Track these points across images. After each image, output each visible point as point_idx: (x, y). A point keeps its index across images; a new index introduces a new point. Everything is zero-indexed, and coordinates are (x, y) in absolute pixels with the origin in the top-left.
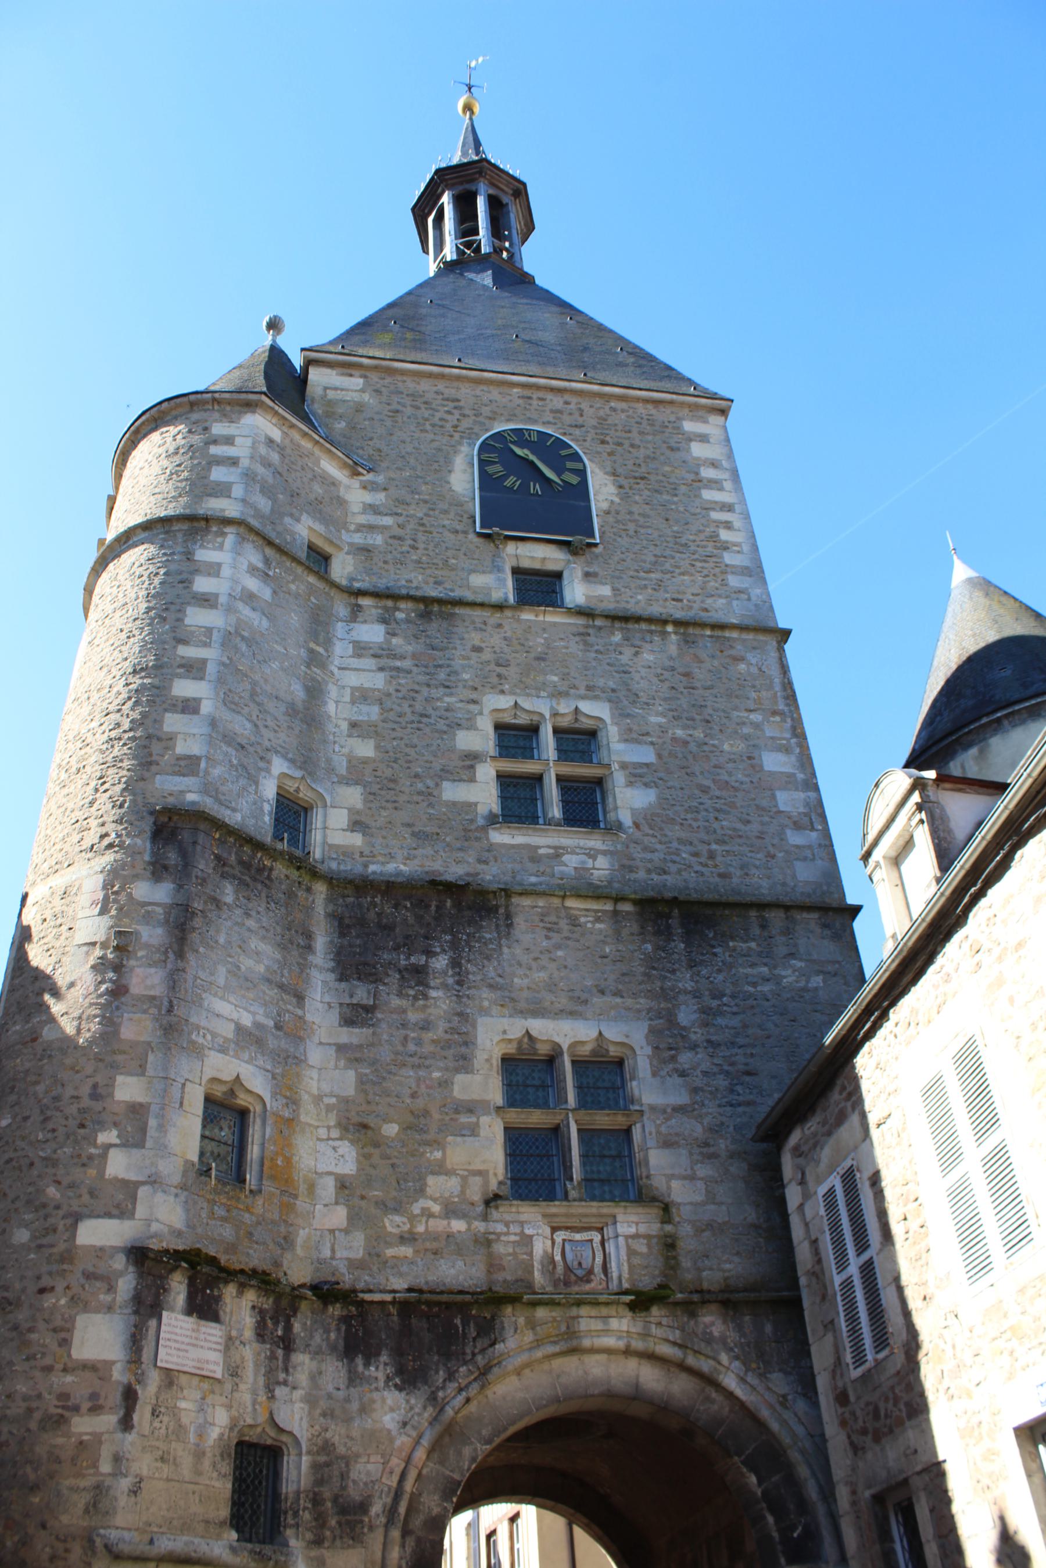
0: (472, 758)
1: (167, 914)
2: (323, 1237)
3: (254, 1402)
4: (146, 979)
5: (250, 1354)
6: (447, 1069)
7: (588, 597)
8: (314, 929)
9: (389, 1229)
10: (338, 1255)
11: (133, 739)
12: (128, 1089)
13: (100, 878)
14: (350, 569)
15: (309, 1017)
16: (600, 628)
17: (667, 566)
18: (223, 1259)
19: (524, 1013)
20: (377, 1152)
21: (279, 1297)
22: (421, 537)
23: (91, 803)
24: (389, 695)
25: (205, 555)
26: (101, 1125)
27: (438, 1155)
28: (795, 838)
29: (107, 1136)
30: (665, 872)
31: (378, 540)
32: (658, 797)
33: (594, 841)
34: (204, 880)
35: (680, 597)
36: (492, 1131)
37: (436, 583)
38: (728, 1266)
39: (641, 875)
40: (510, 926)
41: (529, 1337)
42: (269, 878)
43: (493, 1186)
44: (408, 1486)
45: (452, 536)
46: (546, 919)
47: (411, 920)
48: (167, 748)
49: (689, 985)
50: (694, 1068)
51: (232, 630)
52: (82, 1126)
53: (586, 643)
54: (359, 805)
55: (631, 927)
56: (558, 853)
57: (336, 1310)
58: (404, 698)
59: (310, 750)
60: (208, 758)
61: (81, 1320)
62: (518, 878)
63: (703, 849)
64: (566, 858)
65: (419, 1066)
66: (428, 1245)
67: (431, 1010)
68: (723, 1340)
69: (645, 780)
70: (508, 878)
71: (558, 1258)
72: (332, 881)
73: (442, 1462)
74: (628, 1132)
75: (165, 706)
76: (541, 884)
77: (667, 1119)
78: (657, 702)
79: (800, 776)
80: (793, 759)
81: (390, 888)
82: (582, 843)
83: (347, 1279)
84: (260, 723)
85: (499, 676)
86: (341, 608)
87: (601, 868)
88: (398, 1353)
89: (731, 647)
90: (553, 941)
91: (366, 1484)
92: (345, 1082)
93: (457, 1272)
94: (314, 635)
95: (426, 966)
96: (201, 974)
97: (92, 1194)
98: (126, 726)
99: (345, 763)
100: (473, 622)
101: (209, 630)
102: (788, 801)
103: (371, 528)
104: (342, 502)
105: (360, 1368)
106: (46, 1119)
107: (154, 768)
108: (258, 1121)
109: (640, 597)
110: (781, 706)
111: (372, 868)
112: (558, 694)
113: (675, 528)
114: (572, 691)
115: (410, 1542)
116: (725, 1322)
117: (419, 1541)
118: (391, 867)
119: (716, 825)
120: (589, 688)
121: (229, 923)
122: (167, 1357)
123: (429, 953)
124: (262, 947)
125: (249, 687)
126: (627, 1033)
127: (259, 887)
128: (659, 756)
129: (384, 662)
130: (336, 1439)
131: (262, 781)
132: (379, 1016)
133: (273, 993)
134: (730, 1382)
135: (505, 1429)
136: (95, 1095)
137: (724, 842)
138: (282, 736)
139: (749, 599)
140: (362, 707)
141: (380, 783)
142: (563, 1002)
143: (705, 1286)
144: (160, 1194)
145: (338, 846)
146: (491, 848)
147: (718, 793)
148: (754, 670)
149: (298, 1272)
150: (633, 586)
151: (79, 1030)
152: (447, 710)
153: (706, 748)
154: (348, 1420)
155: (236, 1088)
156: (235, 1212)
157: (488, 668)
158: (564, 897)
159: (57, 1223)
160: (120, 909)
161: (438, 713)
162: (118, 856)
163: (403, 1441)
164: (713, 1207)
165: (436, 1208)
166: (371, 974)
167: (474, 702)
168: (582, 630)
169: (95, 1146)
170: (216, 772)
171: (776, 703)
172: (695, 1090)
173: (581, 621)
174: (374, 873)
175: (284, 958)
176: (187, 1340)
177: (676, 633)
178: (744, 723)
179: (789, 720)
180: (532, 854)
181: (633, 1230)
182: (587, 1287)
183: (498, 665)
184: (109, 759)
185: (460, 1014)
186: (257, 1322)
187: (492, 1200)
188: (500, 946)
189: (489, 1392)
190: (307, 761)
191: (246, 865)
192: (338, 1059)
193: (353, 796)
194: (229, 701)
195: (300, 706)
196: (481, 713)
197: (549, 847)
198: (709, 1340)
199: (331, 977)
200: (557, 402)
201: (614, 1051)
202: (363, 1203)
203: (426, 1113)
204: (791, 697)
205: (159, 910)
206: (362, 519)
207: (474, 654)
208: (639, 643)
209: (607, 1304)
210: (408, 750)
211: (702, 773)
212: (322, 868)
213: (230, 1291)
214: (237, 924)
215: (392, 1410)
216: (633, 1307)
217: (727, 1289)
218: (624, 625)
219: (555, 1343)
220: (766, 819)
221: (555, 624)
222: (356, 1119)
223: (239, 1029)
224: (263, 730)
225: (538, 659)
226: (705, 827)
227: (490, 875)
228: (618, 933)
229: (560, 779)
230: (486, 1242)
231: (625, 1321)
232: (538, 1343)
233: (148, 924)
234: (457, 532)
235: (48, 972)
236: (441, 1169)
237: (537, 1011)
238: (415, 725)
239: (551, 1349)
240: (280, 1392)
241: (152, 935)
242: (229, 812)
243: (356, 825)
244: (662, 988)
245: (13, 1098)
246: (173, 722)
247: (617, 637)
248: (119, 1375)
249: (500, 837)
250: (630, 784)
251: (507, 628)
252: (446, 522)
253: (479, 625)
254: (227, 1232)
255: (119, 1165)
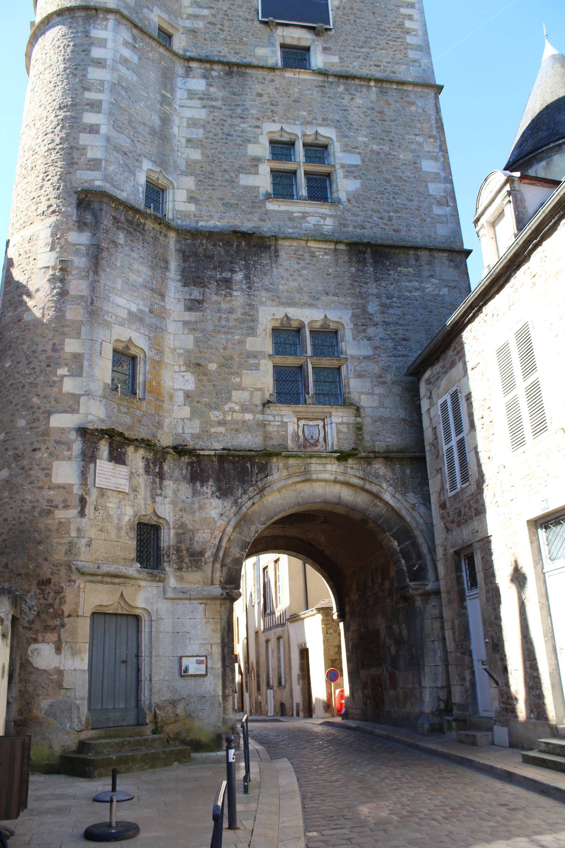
0: (256, 161)
1: (88, 250)
2: (178, 422)
3: (145, 504)
4: (78, 286)
5: (142, 481)
6: (243, 334)
7: (325, 63)
8: (169, 258)
9: (213, 418)
10: (186, 431)
11: (63, 149)
12: (71, 346)
13: (49, 231)
14: (184, 43)
15: (167, 307)
16: (332, 83)
17: (373, 44)
18: (126, 434)
19: (284, 304)
20: (205, 378)
21: (156, 452)
22: (226, 23)
23: (41, 188)
24: (209, 123)
26: (59, 365)
27: (238, 380)
28: (437, 211)
29: (63, 371)
30: (364, 228)
31: (200, 25)
32: (362, 185)
33: (325, 209)
34: (107, 231)
35: (379, 64)
36: (267, 368)
37: (235, 53)
38: (389, 439)
39: (351, 229)
40: (277, 256)
41: (285, 473)
42: (143, 229)
43: (267, 396)
44: (224, 544)
45: (245, 23)
46: (297, 253)
47: (223, 253)
48: (82, 155)
49: (375, 291)
50: (375, 336)
51: (116, 83)
52: (49, 366)
53: (323, 92)
54: (193, 188)
56: (304, 215)
57: (185, 459)
58: (217, 124)
59: (164, 155)
60: (106, 160)
61: (55, 464)
62: (282, 230)
63: (386, 215)
64: (309, 219)
65: (228, 333)
66: (233, 426)
67: (233, 303)
68: (385, 477)
69: (355, 175)
70: (276, 230)
71: (301, 434)
72: (178, 230)
73: (240, 533)
74: (339, 369)
75: (79, 129)
76: (294, 233)
77: (360, 363)
78: (363, 128)
79: (443, 175)
80: (439, 164)
81: (211, 235)
82: (318, 210)
83: (191, 444)
84: (135, 139)
85: (272, 111)
86: (180, 69)
87: (328, 225)
88: (218, 480)
89: (408, 96)
90: (301, 265)
91: (202, 543)
92: (188, 341)
93: (248, 441)
94: (164, 86)
95: (231, 279)
96: (108, 283)
97: (56, 401)
98: (58, 141)
99: (184, 163)
100: (257, 78)
101: (102, 82)
102: (435, 189)
105: (199, 488)
106: (29, 363)
107: (75, 167)
108: (142, 362)
109: (355, 64)
110: (434, 133)
111: (201, 224)
112: (307, 123)
113: (378, 19)
114: (314, 121)
115: (225, 570)
116: (386, 468)
117: (229, 569)
118: (211, 223)
119: (393, 202)
120: (324, 120)
121: (122, 255)
122: (100, 482)
123: (233, 271)
124: (141, 268)
125: (127, 117)
126: (340, 316)
127: (138, 234)
128: (363, 161)
129: (205, 102)
130: (187, 522)
131: (137, 174)
132: (206, 306)
133: (148, 293)
134: (387, 497)
135: (272, 518)
136: (54, 350)
137: (398, 212)
138: (148, 147)
139: (420, 66)
140: (193, 129)
141: (204, 175)
142: (306, 298)
143: (377, 449)
144: (92, 401)
145: (182, 211)
146: (267, 212)
147: (395, 183)
148: (420, 110)
149: (165, 440)
150: (351, 56)
151: (43, 315)
152: (242, 132)
153: (390, 157)
154: (193, 513)
155: (129, 345)
156: (131, 410)
157: (266, 107)
158: (307, 241)
159: (39, 417)
160: (61, 248)
161: (237, 134)
162: (59, 218)
163: (221, 523)
164: (382, 409)
165: (237, 408)
166: (201, 283)
167: (258, 127)
168: (321, 84)
169: (56, 376)
170: (111, 168)
171: (431, 131)
172: (376, 348)
173: (320, 78)
174: (202, 226)
175: (153, 274)
176: (110, 474)
177: (375, 87)
178: (412, 143)
179: (438, 141)
180: (290, 216)
181: (340, 420)
182: (316, 449)
183: (272, 105)
184: (49, 161)
185: (250, 305)
186: (180, 762)
187: (266, 404)
188: (272, 268)
189: (264, 500)
190: (163, 161)
191: (130, 222)
192: (184, 329)
193: (189, 182)
194: (116, 126)
195: (158, 129)
196: (262, 134)
197: (299, 212)
198: (377, 476)
199: (179, 284)
201: (333, 326)
202: (199, 405)
203: (231, 358)
204: (440, 127)
205: (83, 248)
207: (257, 98)
208: (353, 92)
209: (325, 457)
210: (220, 156)
211: (387, 171)
212: (173, 224)
213: (130, 450)
214: (126, 255)
215: (215, 508)
216: (339, 459)
217: (388, 451)
218: (345, 81)
219: (298, 476)
220: (422, 199)
221: (305, 80)
222: (194, 361)
223: (130, 313)
224: (137, 144)
225: (295, 101)
226: (388, 203)
227: (267, 228)
228: (337, 261)
229: (306, 173)
230: (263, 425)
231: (334, 466)
232: (290, 476)
233: (77, 256)
234: (248, 20)
235: (24, 283)
236: (239, 387)
237: (292, 304)
238: (224, 141)
239: (296, 479)
240: (158, 499)
241: (80, 262)
242: (119, 192)
243: (191, 199)
244: (360, 292)
245: (11, 352)
246: (84, 139)
247: (341, 89)
248: (77, 491)
249: (273, 206)
250: (346, 177)
251: (277, 82)
252: (241, 14)
253: (260, 80)
254: (128, 420)
255: (69, 386)
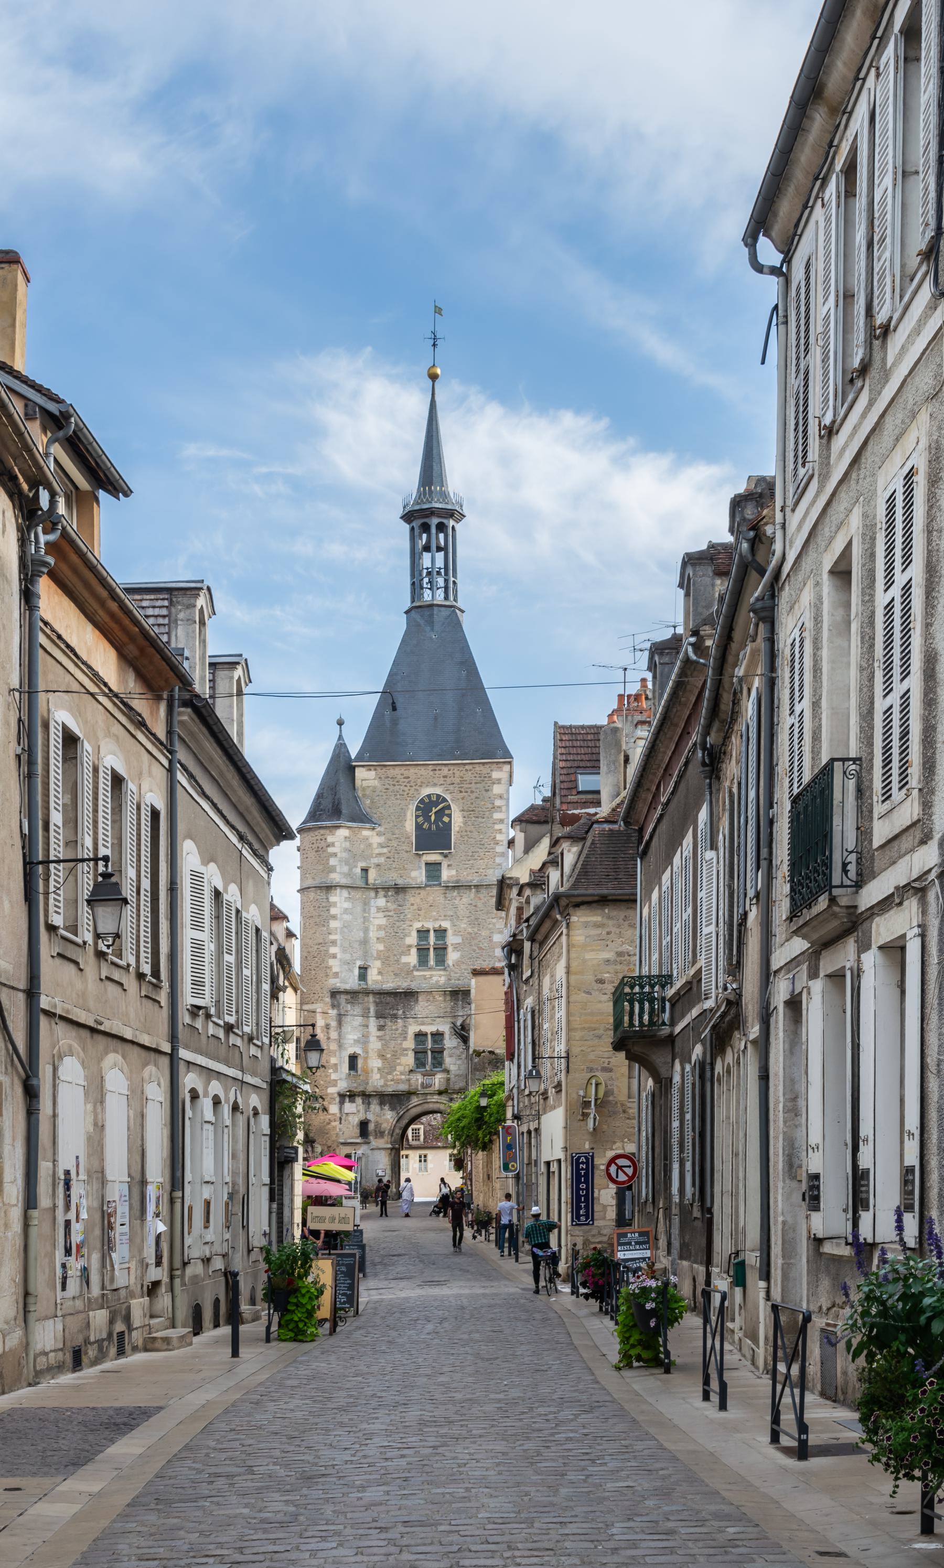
0: (410, 946)
2: (376, 1082)
25: (333, 899)
31: (382, 860)
36: (411, 1055)
55: (448, 998)
86: (372, 894)
93: (403, 1087)
94: (364, 911)
103: (380, 854)
104: (370, 845)
141: (386, 959)
149: (370, 1089)
180: (425, 978)
193: (378, 964)
194: (344, 951)
200: (445, 769)
206: (377, 851)
227: (414, 986)
230: (409, 1080)
236: (399, 1064)
237: (423, 1024)
241: (334, 1024)
243: (380, 973)
249: (416, 973)
255: (333, 1077)
